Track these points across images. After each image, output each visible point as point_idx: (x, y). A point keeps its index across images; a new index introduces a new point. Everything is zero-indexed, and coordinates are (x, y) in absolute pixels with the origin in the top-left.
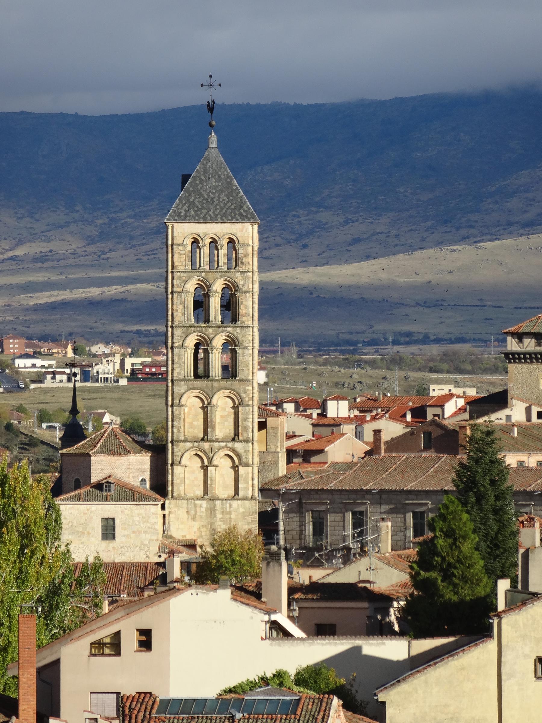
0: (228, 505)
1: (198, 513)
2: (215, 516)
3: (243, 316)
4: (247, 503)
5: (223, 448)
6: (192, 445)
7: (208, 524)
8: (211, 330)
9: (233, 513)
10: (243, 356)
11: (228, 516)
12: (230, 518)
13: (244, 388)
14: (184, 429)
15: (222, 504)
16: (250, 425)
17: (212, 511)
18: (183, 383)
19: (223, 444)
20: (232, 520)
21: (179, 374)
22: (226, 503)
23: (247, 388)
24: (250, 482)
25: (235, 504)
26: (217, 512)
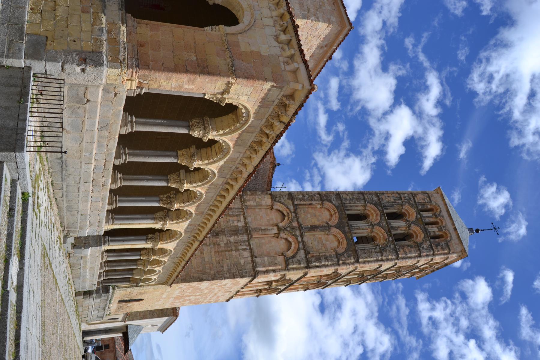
0: (244, 247)
1: (231, 219)
2: (231, 235)
3: (403, 249)
4: (250, 266)
5: (297, 239)
6: (292, 211)
7: (222, 229)
8: (385, 224)
9: (238, 253)
10: (376, 252)
11: (234, 248)
12: (232, 250)
13: (351, 256)
14: (303, 204)
15: (244, 242)
16: (323, 263)
17: (236, 232)
18: (340, 202)
19: (299, 239)
20: (230, 253)
21: (346, 199)
22: (246, 245)
23: (352, 258)
24: (271, 268)
25: (247, 254)
26: (236, 237)
